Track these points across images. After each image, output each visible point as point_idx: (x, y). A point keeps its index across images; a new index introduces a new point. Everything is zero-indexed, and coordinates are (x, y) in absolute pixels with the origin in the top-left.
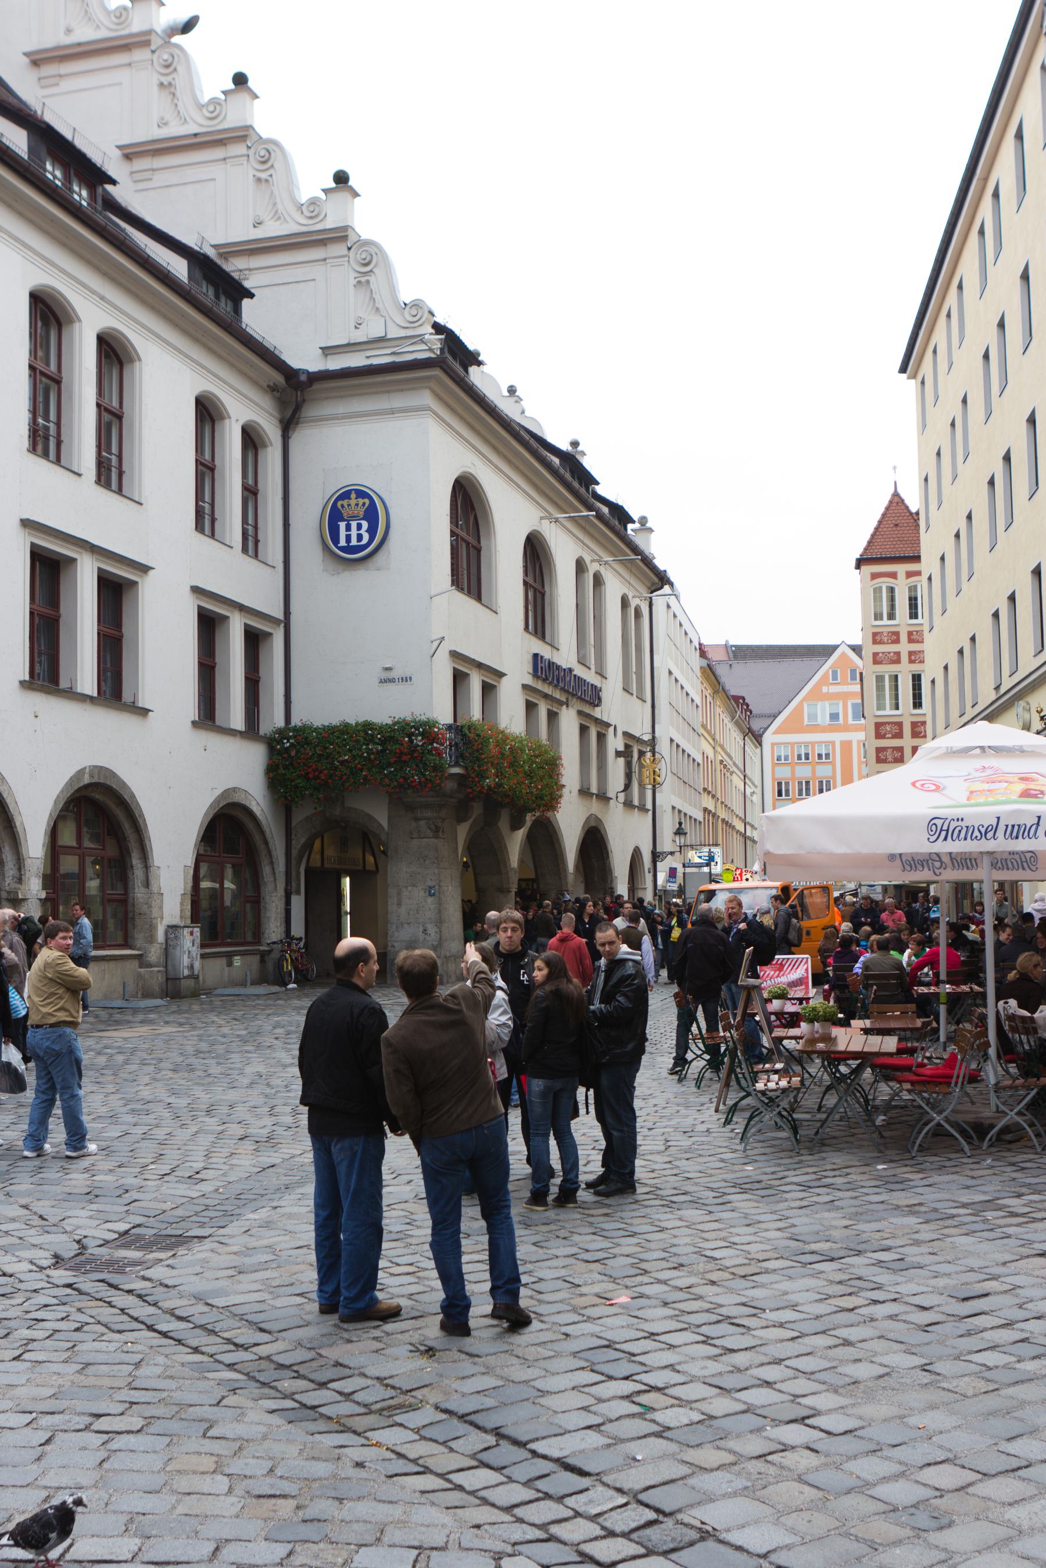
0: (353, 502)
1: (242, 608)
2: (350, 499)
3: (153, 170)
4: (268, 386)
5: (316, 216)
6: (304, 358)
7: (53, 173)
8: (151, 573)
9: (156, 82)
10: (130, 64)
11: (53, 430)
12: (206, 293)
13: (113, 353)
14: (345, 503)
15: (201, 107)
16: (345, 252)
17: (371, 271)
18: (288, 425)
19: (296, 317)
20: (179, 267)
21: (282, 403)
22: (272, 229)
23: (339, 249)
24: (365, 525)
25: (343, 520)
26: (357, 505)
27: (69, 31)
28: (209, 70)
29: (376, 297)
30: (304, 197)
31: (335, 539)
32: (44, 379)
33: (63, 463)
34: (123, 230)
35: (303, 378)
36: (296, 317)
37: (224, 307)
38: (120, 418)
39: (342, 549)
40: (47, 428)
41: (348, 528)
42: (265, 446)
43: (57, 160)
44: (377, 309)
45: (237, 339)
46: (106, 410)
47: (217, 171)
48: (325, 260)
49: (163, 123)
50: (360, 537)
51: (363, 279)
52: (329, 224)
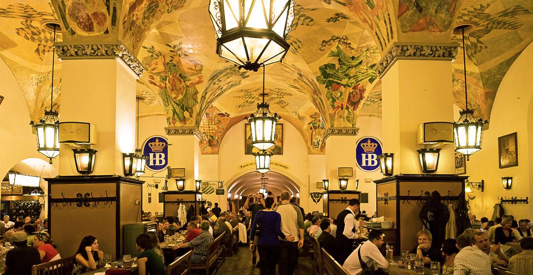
0: (369, 144)
2: (367, 143)
14: (365, 144)
25: (364, 153)
41: (367, 157)
50: (373, 162)
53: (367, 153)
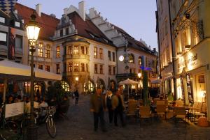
18: (117, 51)
19: (117, 43)
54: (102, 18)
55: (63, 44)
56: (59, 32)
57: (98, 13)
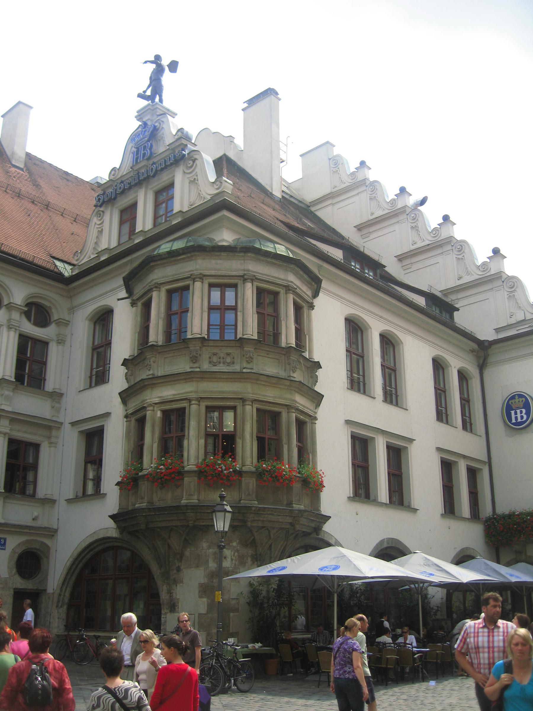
0: (517, 400)
1: (464, 457)
3: (412, 263)
4: (470, 350)
5: (487, 270)
6: (486, 334)
7: (355, 266)
8: (414, 442)
9: (410, 227)
10: (398, 222)
11: (361, 380)
12: (435, 311)
13: (388, 342)
14: (513, 401)
15: (430, 233)
16: (501, 283)
17: (515, 290)
18: (482, 367)
20: (421, 301)
21: (478, 357)
22: (467, 279)
23: (499, 283)
24: (524, 411)
26: (519, 401)
27: (372, 214)
28: (432, 217)
29: (519, 302)
30: (479, 262)
31: (510, 420)
32: (355, 356)
33: (367, 394)
34: (393, 288)
35: (486, 344)
36: (480, 318)
37: (445, 316)
38: (395, 371)
39: (513, 424)
40: (359, 379)
41: (516, 413)
42: (471, 378)
43: (356, 260)
44: (520, 307)
45: (439, 322)
46: (388, 368)
47: (439, 259)
48: (492, 289)
49: (414, 243)
50: (522, 417)
51: (511, 295)
52: (493, 272)
53: (515, 410)
54: (374, 187)
55: (129, 283)
56: (111, 219)
57: (353, 166)
